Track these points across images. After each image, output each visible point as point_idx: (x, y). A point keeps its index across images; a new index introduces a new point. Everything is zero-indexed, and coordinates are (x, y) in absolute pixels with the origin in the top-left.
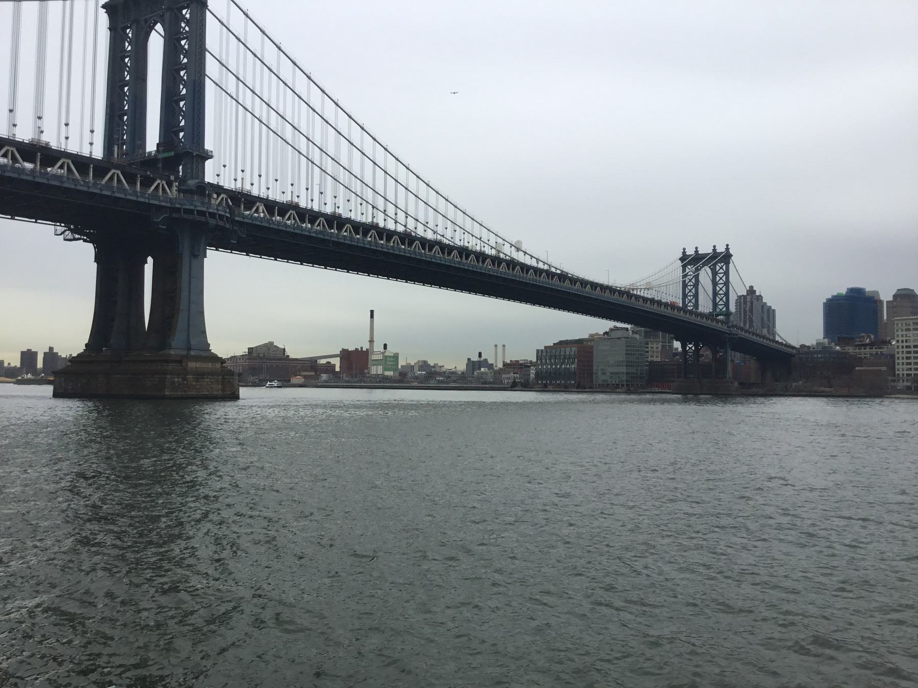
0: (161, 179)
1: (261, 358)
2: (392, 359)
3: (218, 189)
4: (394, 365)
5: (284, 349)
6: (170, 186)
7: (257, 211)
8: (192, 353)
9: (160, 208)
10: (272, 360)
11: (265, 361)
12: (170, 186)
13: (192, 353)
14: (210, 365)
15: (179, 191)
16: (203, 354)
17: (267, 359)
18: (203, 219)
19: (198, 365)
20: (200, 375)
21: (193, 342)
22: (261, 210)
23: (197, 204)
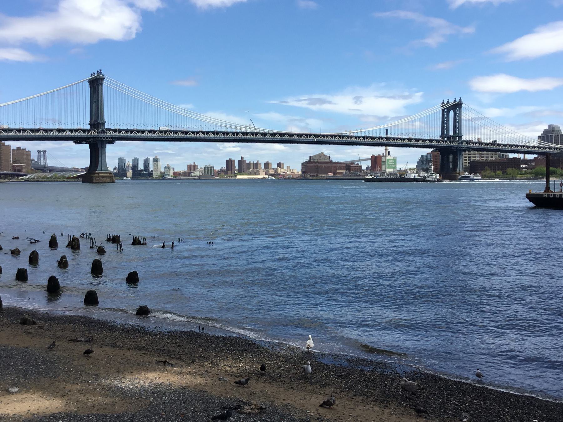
0: (92, 130)
1: (315, 163)
2: (392, 161)
3: (109, 130)
4: (393, 165)
5: (330, 157)
6: (95, 132)
7: (122, 133)
8: (102, 171)
9: (90, 138)
10: (322, 163)
11: (317, 164)
12: (95, 132)
13: (102, 171)
14: (106, 174)
15: (97, 133)
16: (107, 171)
17: (319, 163)
18: (101, 139)
19: (102, 174)
20: (103, 177)
21: (103, 169)
22: (124, 133)
23: (102, 135)
